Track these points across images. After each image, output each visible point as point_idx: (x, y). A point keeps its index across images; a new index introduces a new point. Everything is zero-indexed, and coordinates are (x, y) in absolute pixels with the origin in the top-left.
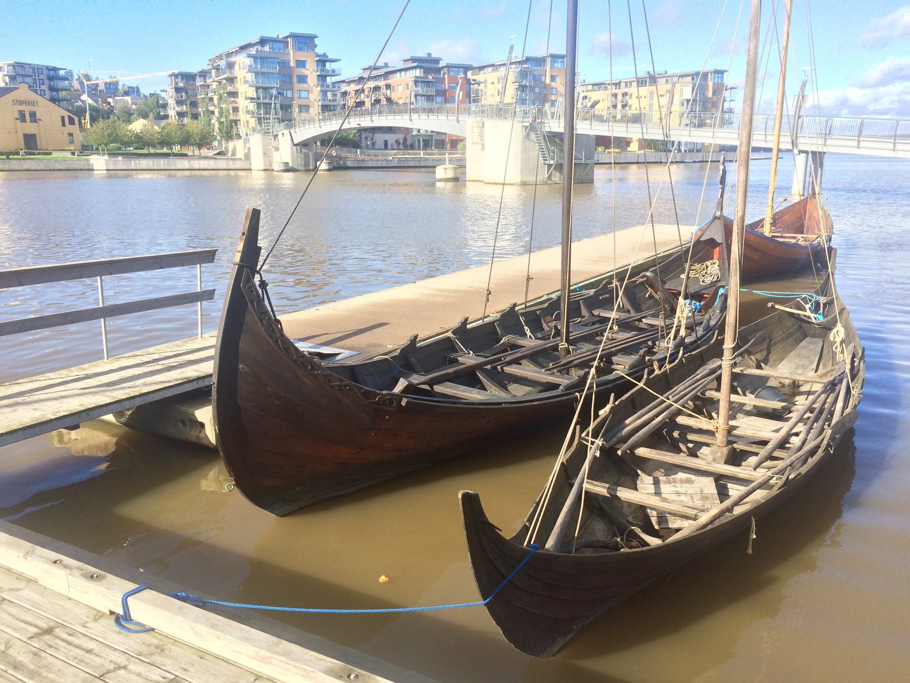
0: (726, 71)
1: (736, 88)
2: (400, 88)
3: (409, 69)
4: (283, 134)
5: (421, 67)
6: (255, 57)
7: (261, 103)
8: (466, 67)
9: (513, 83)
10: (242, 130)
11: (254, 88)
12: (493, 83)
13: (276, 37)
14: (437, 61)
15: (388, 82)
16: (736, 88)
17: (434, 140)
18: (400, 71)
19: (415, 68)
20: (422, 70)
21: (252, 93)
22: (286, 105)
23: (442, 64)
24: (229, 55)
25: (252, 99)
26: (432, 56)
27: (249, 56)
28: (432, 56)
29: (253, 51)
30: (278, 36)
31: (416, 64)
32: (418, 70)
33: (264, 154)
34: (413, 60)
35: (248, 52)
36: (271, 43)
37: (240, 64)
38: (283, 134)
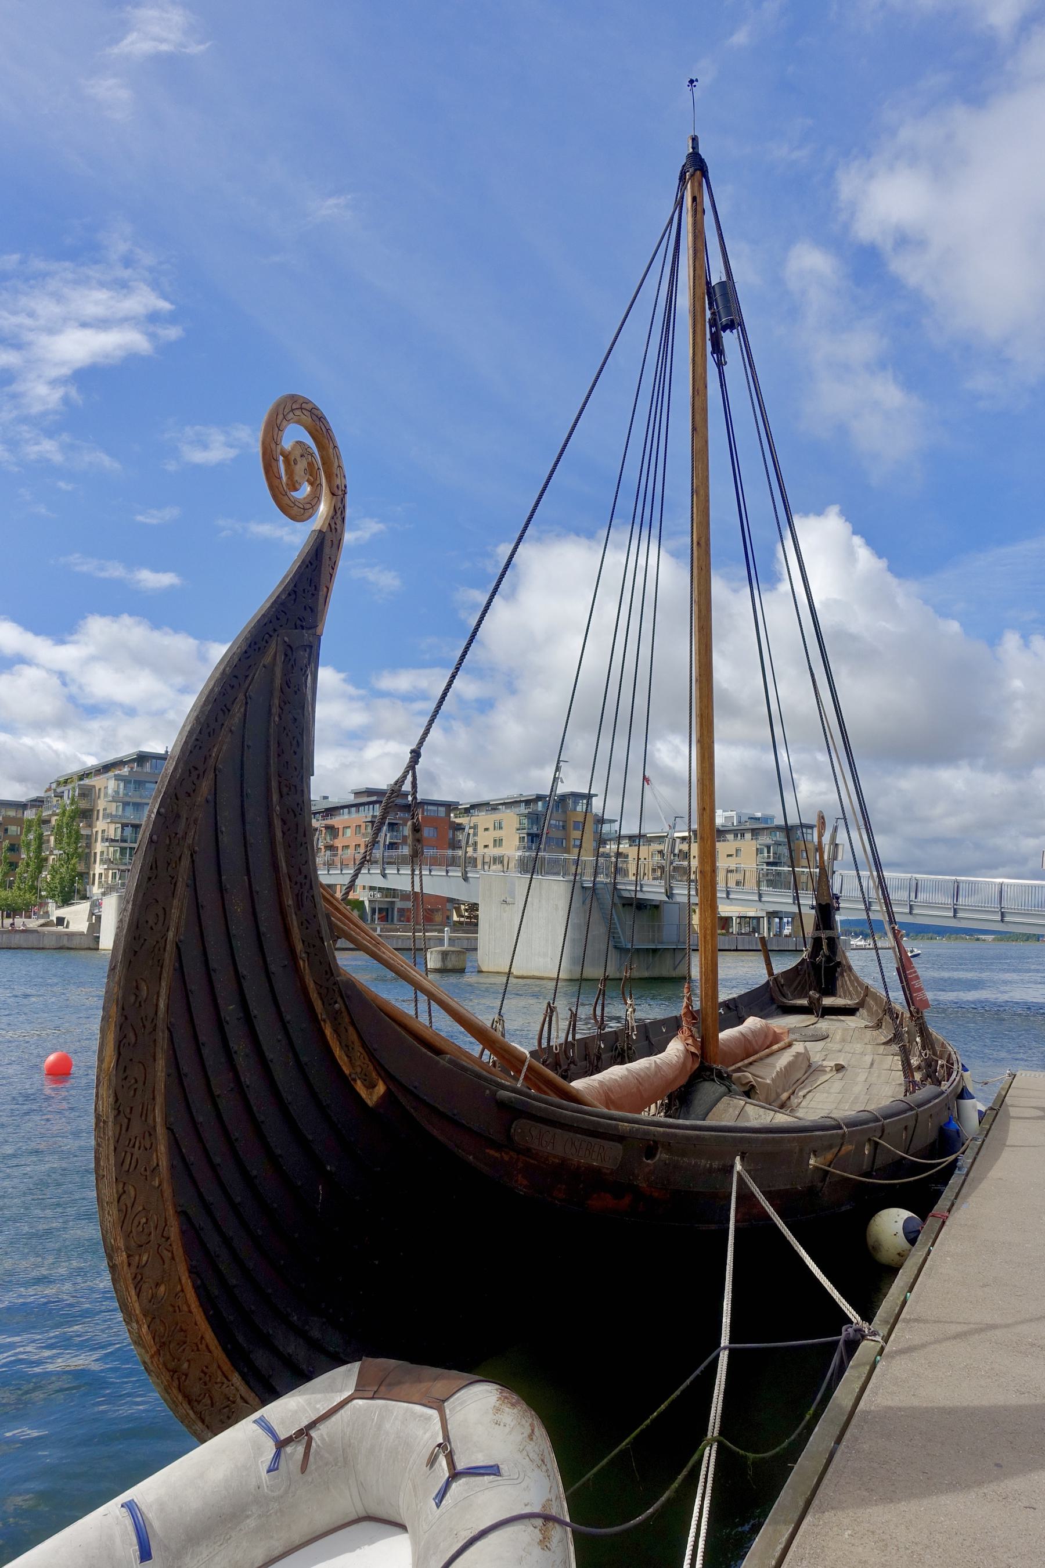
2: (349, 832)
6: (125, 780)
7: (126, 848)
8: (450, 805)
9: (518, 830)
11: (120, 825)
12: (486, 829)
13: (163, 752)
15: (329, 822)
17: (396, 909)
24: (84, 775)
25: (113, 840)
27: (118, 778)
29: (125, 771)
31: (374, 798)
34: (369, 792)
35: (116, 773)
36: (154, 761)
37: (100, 789)
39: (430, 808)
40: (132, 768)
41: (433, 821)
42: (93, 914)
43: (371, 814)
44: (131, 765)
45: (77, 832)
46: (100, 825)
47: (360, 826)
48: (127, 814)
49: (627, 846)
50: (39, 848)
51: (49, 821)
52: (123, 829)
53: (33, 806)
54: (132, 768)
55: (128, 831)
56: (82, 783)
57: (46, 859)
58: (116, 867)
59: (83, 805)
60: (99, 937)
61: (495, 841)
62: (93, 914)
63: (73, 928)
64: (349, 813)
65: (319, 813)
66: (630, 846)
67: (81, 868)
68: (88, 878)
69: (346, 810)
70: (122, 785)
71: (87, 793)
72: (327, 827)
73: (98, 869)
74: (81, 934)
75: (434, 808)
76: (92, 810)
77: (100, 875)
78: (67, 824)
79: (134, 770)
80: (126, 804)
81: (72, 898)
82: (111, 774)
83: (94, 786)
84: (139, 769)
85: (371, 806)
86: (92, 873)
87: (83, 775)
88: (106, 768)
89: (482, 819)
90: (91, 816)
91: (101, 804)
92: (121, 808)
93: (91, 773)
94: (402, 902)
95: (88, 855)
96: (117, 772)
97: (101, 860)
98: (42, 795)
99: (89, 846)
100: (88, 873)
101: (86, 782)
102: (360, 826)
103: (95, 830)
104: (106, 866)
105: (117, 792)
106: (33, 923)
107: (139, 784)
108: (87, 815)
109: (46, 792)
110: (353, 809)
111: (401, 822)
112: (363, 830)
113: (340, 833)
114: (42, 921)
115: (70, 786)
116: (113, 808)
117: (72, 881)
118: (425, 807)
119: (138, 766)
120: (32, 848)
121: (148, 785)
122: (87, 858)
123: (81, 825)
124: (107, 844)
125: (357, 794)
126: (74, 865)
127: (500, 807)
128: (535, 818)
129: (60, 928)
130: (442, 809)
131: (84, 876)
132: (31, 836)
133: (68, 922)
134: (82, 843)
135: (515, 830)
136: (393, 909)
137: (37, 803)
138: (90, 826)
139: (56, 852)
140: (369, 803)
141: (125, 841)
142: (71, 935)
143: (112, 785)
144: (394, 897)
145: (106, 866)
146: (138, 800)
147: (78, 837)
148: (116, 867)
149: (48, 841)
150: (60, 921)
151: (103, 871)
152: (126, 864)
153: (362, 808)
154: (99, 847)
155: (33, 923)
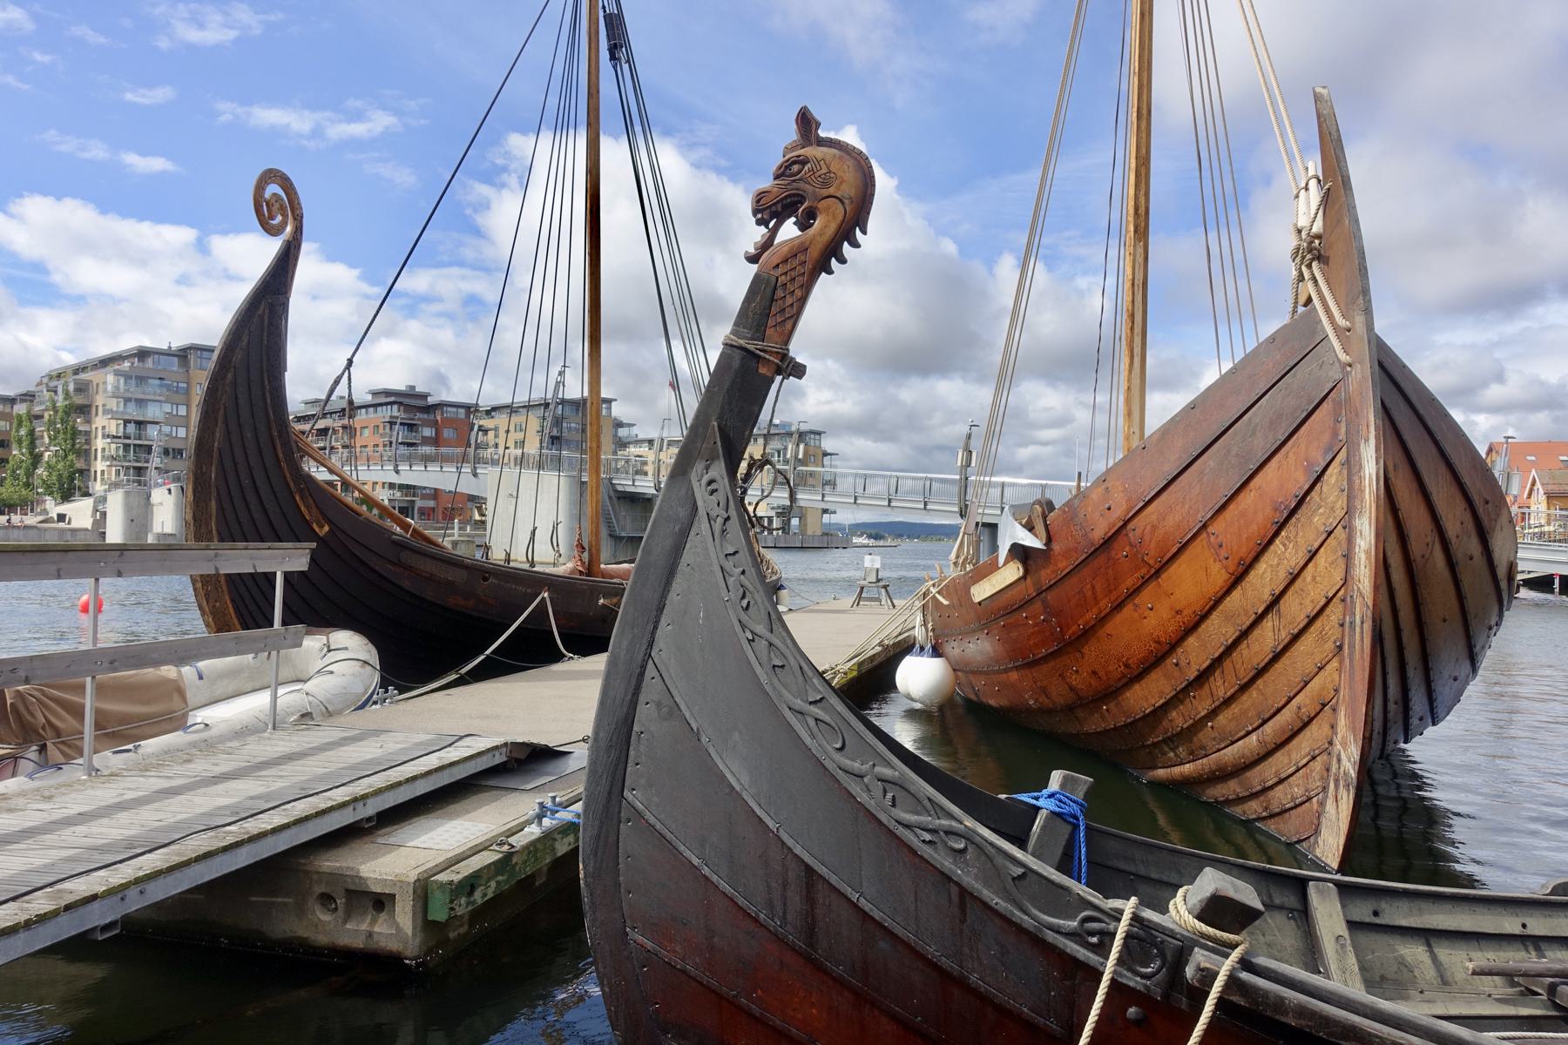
0: (824, 433)
1: (837, 454)
2: (366, 432)
3: (381, 405)
4: (170, 490)
5: (400, 404)
6: (127, 377)
7: (129, 445)
8: (470, 408)
10: (98, 487)
11: (122, 422)
13: (166, 347)
14: (424, 396)
16: (837, 454)
18: (366, 407)
19: (391, 403)
20: (402, 408)
21: (114, 427)
22: (173, 450)
23: (431, 400)
24: (79, 369)
26: (417, 390)
27: (117, 373)
28: (417, 390)
29: (127, 364)
30: (170, 347)
31: (392, 399)
32: (395, 407)
33: (132, 521)
34: (387, 393)
35: (117, 367)
36: (156, 356)
37: (97, 384)
38: (170, 490)
39: (449, 409)
40: (133, 363)
41: (451, 422)
42: (97, 511)
43: (389, 414)
44: (132, 360)
45: (73, 428)
46: (100, 421)
47: (378, 426)
48: (129, 410)
49: (647, 449)
50: (32, 445)
51: (42, 417)
52: (125, 426)
53: (23, 401)
54: (133, 363)
55: (131, 428)
56: (76, 377)
57: (41, 455)
58: (119, 463)
59: (79, 400)
60: (104, 533)
61: (516, 442)
62: (97, 511)
63: (74, 525)
64: (367, 412)
65: (336, 413)
66: (650, 449)
67: (80, 465)
68: (89, 476)
69: (363, 411)
70: (122, 380)
71: (82, 388)
72: (344, 427)
73: (100, 465)
74: (87, 530)
75: (454, 410)
76: (89, 406)
77: (103, 472)
78: (62, 420)
79: (136, 364)
80: (127, 400)
81: (72, 495)
82: (109, 369)
83: (91, 382)
84: (141, 365)
85: (389, 407)
86: (93, 470)
87: (78, 369)
88: (105, 362)
89: (501, 420)
90: (89, 413)
91: (99, 400)
92: (122, 405)
93: (87, 367)
94: (422, 501)
95: (87, 452)
96: (117, 367)
97: (103, 457)
98: (32, 389)
99: (88, 442)
100: (89, 470)
101: (83, 376)
102: (378, 426)
103: (94, 426)
104: (108, 463)
105: (117, 388)
106: (31, 520)
107: (141, 380)
108: (85, 410)
109: (37, 386)
110: (371, 410)
111: (420, 423)
112: (381, 431)
113: (358, 434)
114: (41, 518)
115: (62, 381)
116: (113, 404)
117: (72, 479)
118: (445, 409)
119: (139, 361)
120: (25, 444)
121: (151, 381)
122: (86, 454)
123: (79, 420)
124: (109, 440)
125: (375, 394)
126: (72, 461)
127: (521, 410)
128: (558, 422)
129: (61, 525)
130: (462, 411)
131: (84, 473)
132: (23, 432)
133: (70, 519)
134: (80, 440)
135: (535, 432)
136: (413, 508)
137: (29, 397)
138: (89, 422)
139: (52, 448)
140: (387, 404)
141: (129, 438)
142: (74, 531)
143: (110, 378)
144: (414, 496)
145: (108, 463)
146: (142, 397)
147: (75, 433)
148: (119, 463)
149: (42, 437)
150: (61, 517)
151: (105, 468)
152: (130, 461)
153: (379, 409)
154: (100, 443)
155: (31, 520)
